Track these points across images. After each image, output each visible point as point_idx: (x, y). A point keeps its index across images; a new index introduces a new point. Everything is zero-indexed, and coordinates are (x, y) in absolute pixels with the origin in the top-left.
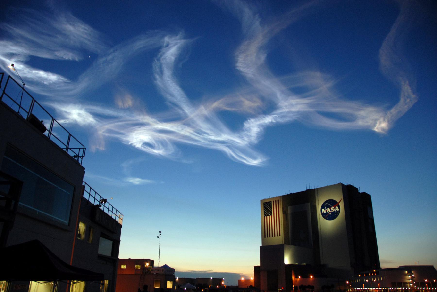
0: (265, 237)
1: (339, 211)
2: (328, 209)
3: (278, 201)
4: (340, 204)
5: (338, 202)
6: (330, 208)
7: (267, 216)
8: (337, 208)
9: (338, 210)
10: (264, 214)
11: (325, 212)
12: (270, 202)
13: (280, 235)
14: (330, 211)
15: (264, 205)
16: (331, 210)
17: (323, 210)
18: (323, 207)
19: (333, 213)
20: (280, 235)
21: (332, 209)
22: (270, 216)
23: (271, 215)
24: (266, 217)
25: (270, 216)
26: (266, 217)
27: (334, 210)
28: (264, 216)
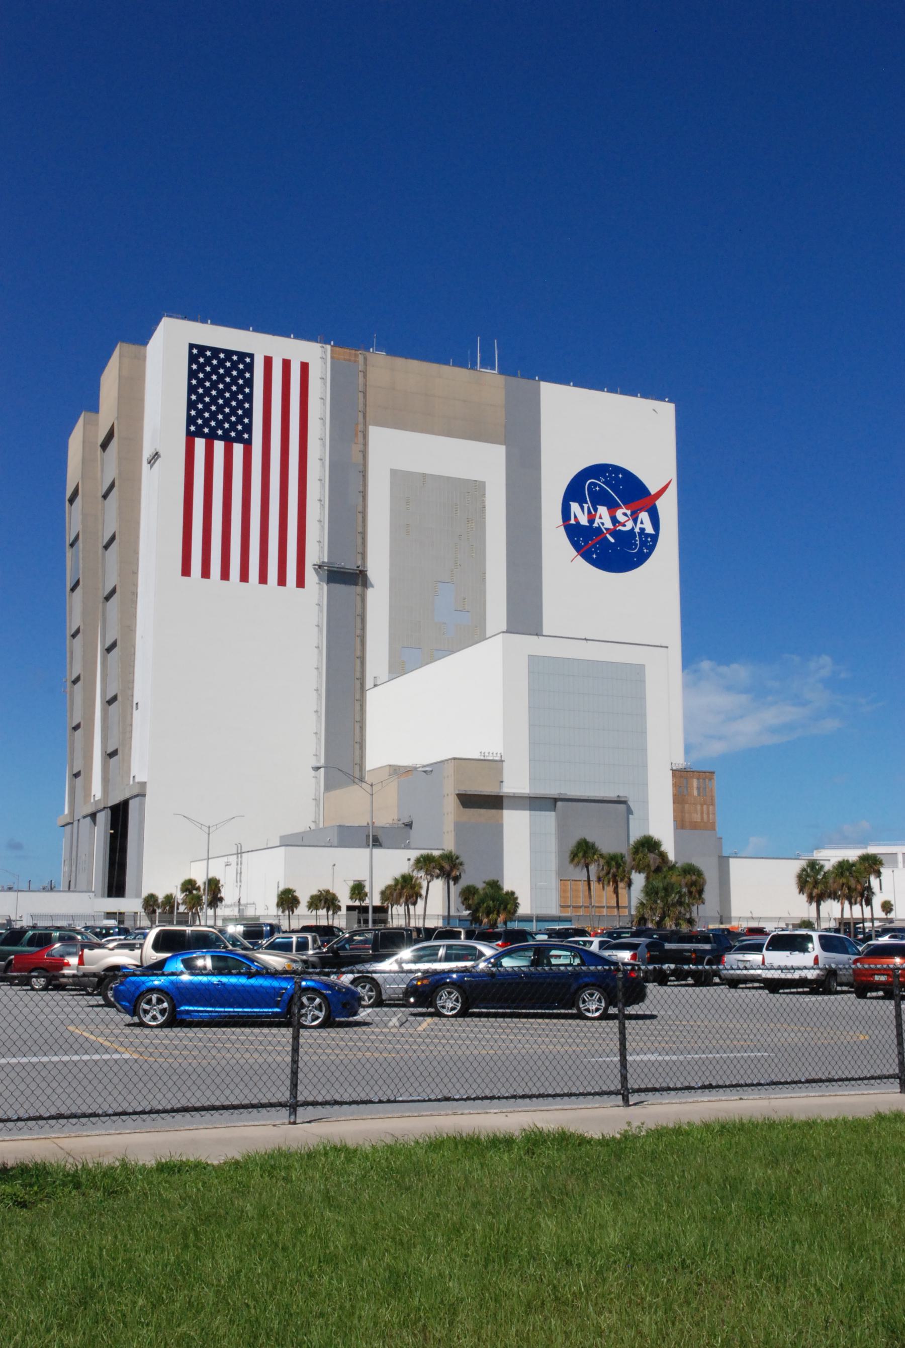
0: (186, 571)
1: (655, 538)
2: (603, 510)
3: (305, 367)
4: (658, 503)
5: (653, 491)
6: (612, 507)
7: (211, 438)
8: (644, 516)
9: (649, 530)
10: (190, 420)
11: (584, 521)
12: (245, 360)
13: (301, 583)
14: (609, 524)
15: (192, 359)
16: (614, 520)
17: (575, 507)
18: (575, 491)
19: (625, 538)
20: (301, 583)
21: (619, 515)
22: (238, 449)
23: (248, 444)
24: (200, 444)
25: (238, 449)
26: (200, 444)
27: (629, 525)
28: (190, 437)
